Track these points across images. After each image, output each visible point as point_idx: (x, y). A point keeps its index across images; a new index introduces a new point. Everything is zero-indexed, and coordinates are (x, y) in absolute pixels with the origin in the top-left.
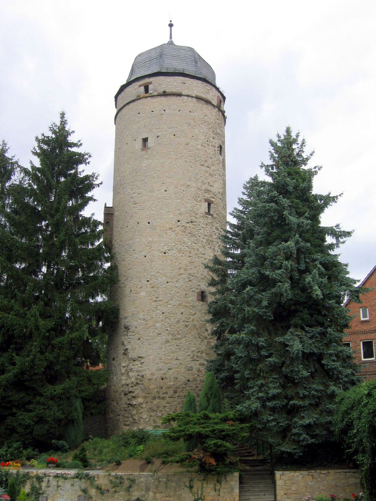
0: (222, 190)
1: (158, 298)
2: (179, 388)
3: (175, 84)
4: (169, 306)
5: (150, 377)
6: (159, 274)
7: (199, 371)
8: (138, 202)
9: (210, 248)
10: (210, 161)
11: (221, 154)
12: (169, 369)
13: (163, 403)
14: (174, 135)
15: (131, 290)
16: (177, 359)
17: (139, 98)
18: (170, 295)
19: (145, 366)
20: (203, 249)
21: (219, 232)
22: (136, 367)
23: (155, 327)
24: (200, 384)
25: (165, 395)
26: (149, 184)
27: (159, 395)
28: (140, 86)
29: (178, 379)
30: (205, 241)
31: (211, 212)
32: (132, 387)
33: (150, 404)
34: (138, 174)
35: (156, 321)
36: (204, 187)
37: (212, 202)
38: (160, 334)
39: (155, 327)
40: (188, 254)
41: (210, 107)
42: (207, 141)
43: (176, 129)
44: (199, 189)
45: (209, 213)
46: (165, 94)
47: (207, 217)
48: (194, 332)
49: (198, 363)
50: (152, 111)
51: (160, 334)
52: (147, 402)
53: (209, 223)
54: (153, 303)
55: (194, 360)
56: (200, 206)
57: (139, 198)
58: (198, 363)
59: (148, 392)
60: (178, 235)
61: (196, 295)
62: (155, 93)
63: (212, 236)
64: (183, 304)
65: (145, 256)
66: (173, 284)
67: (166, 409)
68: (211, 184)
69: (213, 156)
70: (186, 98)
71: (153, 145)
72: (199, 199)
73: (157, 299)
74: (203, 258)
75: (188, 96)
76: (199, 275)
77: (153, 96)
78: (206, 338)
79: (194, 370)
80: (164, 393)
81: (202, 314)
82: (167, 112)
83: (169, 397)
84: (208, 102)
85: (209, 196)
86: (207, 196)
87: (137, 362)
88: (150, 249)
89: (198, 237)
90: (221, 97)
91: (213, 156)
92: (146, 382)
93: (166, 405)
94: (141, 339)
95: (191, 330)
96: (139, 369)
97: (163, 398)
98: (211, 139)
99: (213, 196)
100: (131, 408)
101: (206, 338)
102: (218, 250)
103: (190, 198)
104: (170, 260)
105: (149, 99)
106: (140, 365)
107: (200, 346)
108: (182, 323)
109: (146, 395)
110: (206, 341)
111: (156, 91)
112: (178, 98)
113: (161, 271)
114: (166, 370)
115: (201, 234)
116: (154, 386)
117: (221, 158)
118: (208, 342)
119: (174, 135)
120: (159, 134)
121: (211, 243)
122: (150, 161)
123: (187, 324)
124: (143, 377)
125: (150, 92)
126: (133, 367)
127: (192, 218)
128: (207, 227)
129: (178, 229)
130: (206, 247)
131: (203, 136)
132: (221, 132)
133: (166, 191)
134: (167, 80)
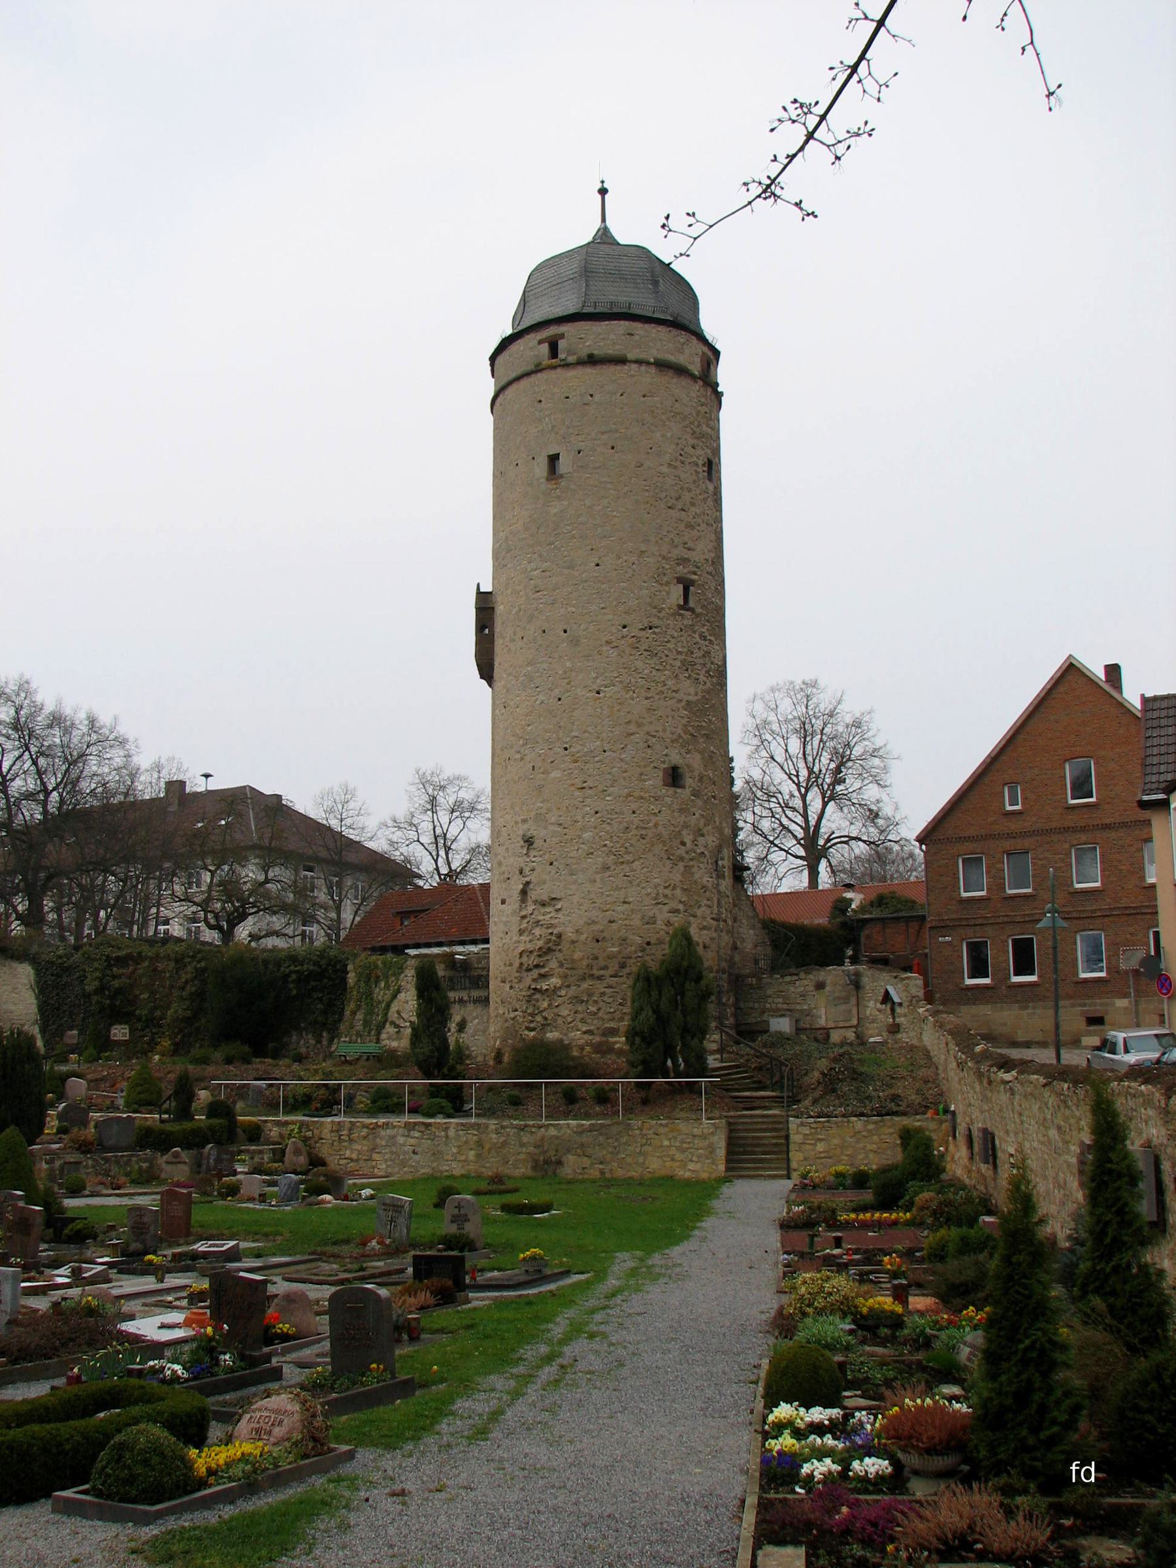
0: (713, 555)
2: (630, 958)
3: (612, 336)
4: (608, 798)
5: (573, 936)
6: (586, 735)
9: (689, 677)
10: (687, 497)
11: (710, 479)
12: (611, 922)
13: (600, 987)
14: (613, 448)
15: (533, 767)
16: (625, 902)
17: (538, 369)
18: (609, 777)
20: (674, 682)
21: (707, 643)
22: (547, 917)
23: (581, 841)
25: (602, 972)
27: (591, 972)
29: (628, 941)
30: (678, 664)
31: (691, 604)
32: (540, 956)
33: (573, 991)
34: (542, 530)
35: (583, 829)
36: (676, 553)
37: (692, 583)
38: (592, 853)
40: (644, 694)
41: (685, 381)
42: (681, 455)
43: (618, 435)
44: (664, 558)
45: (685, 606)
46: (592, 360)
47: (680, 615)
48: (659, 848)
49: (666, 908)
50: (567, 398)
51: (592, 853)
52: (568, 986)
53: (686, 626)
54: (577, 793)
55: (659, 903)
56: (668, 593)
58: (666, 908)
60: (623, 654)
61: (661, 774)
62: (571, 359)
63: (692, 653)
64: (636, 794)
65: (560, 699)
66: (615, 755)
67: (605, 998)
68: (690, 544)
69: (692, 487)
70: (634, 366)
71: (570, 470)
72: (665, 579)
75: (639, 362)
76: (668, 734)
77: (566, 365)
78: (682, 859)
79: (659, 922)
80: (602, 969)
81: (673, 811)
82: (597, 398)
83: (611, 976)
84: (680, 371)
85: (686, 571)
86: (681, 570)
87: (548, 909)
88: (568, 684)
89: (664, 658)
90: (710, 354)
91: (692, 487)
92: (565, 946)
93: (606, 990)
94: (555, 863)
95: (653, 845)
97: (600, 978)
98: (690, 450)
99: (695, 569)
100: (537, 996)
101: (682, 859)
102: (705, 679)
103: (646, 578)
104: (608, 707)
105: (559, 370)
107: (671, 876)
108: (634, 832)
110: (681, 864)
111: (574, 354)
112: (619, 368)
113: (590, 729)
114: (605, 922)
115: (670, 650)
117: (711, 487)
118: (686, 867)
119: (613, 448)
120: (581, 445)
122: (566, 503)
123: (644, 832)
125: (562, 356)
126: (541, 918)
127: (651, 620)
129: (623, 642)
131: (673, 446)
132: (709, 430)
133: (598, 565)
134: (594, 328)
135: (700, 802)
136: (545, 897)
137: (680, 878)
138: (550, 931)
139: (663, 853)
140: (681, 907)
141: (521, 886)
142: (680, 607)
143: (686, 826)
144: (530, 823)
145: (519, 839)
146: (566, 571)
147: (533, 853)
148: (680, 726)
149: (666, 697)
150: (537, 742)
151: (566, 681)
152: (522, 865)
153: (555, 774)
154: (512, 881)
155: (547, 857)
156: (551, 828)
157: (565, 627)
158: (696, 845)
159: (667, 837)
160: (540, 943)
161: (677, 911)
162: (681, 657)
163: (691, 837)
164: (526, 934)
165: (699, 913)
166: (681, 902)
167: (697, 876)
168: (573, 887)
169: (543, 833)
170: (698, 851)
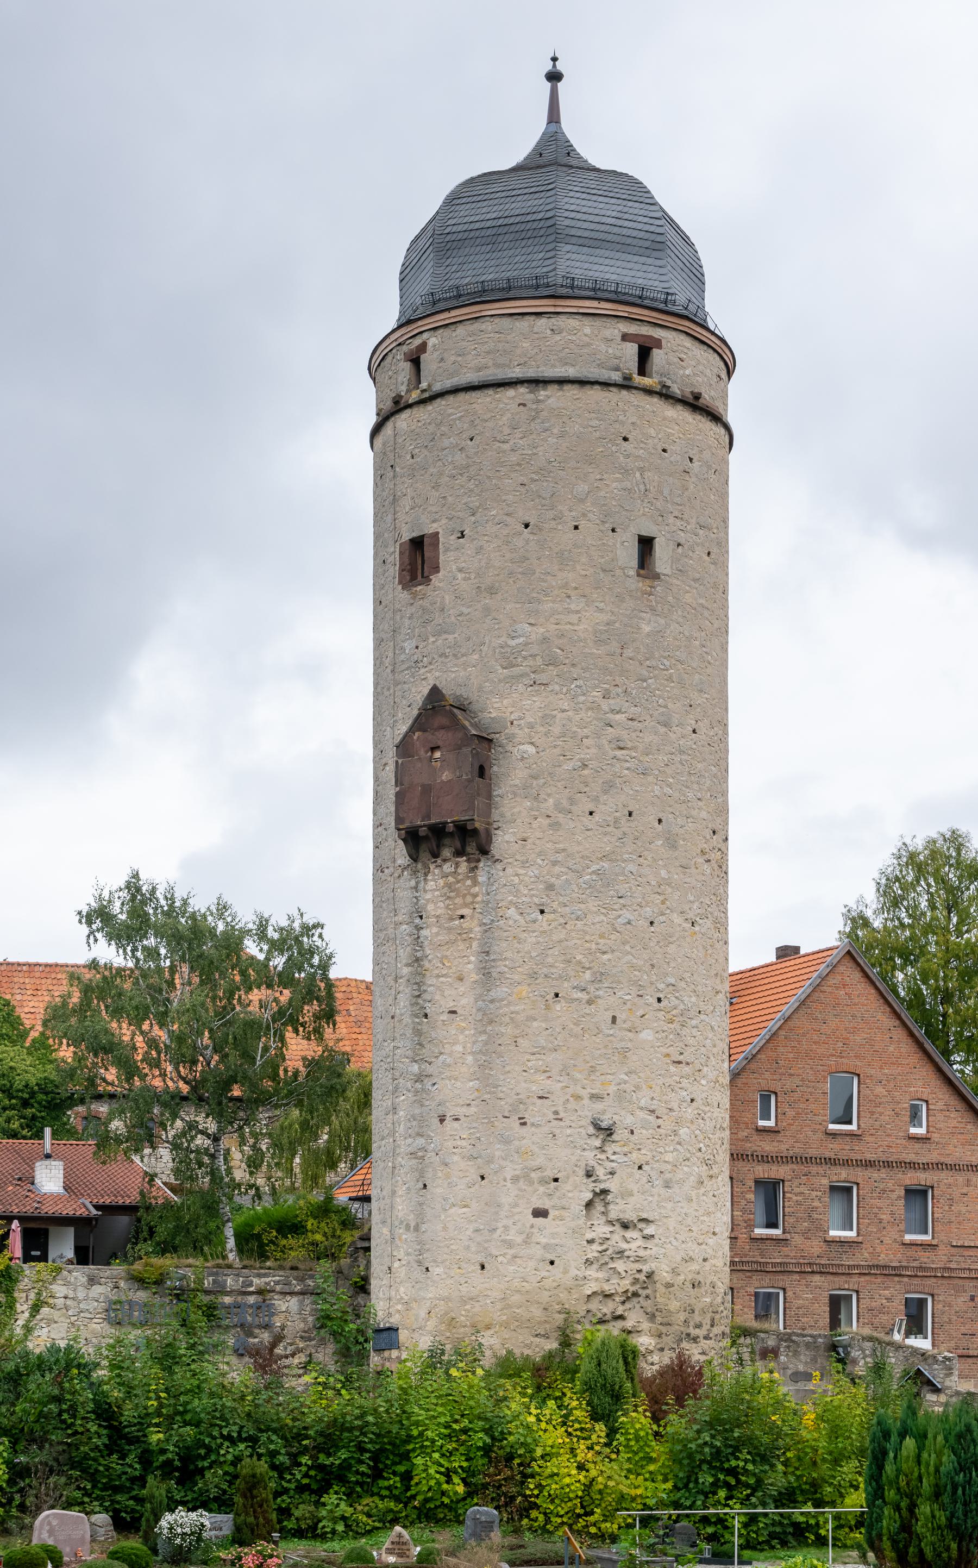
1: (681, 1054)
6: (683, 984)
8: (629, 745)
17: (626, 385)
19: (656, 1245)
22: (633, 1245)
23: (677, 1139)
26: (660, 697)
28: (625, 337)
34: (628, 652)
38: (688, 1160)
39: (677, 1139)
50: (664, 451)
52: (662, 1350)
54: (673, 1069)
57: (634, 735)
59: (665, 1320)
65: (652, 923)
73: (681, 1058)
87: (629, 1234)
88: (663, 902)
94: (645, 1167)
96: (642, 1253)
97: (695, 1340)
105: (655, 400)
106: (640, 1242)
109: (660, 1327)
116: (678, 1304)
124: (650, 1276)
126: (624, 1246)
136: (631, 1216)
138: (638, 1266)
141: (589, 1196)
144: (608, 1101)
145: (586, 1122)
146: (662, 730)
147: (610, 1148)
150: (620, 982)
151: (662, 898)
152: (592, 1163)
153: (647, 1035)
154: (565, 1187)
155: (635, 1155)
156: (642, 1115)
157: (660, 815)
160: (626, 1284)
164: (595, 1266)
168: (669, 1205)
169: (629, 1120)
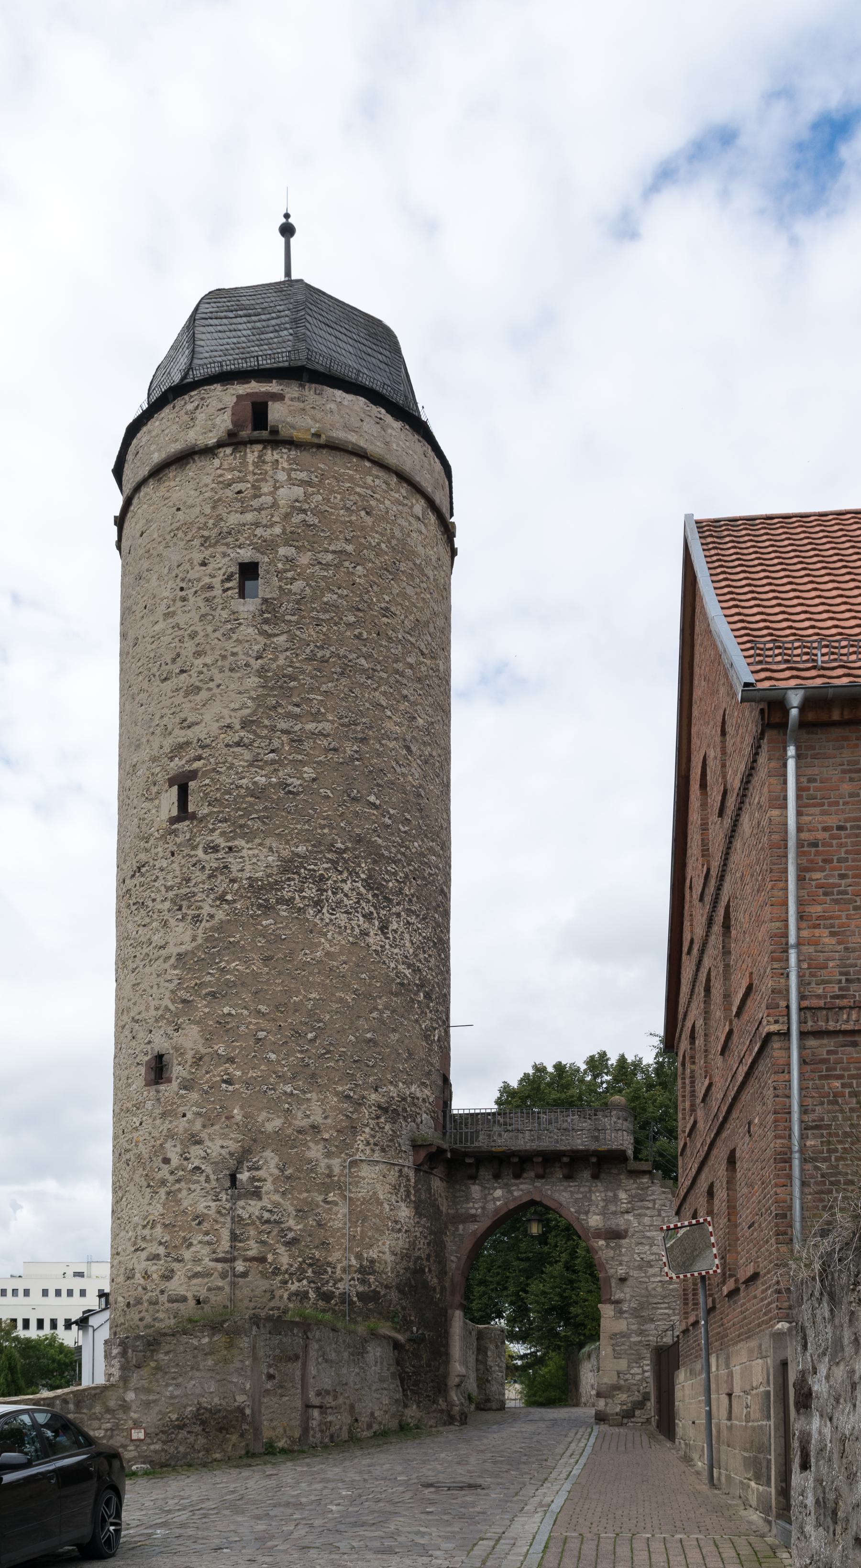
7: (147, 1276)
9: (183, 919)
24: (147, 1311)
30: (167, 905)
49: (144, 1255)
58: (144, 1255)
74: (161, 960)
85: (183, 762)
101: (163, 1182)
121: (185, 904)
128: (173, 862)
130: (172, 922)
135: (194, 1096)
137: (161, 1210)
139: (143, 1179)
140: (161, 1250)
142: (173, 821)
143: (171, 1135)
148: (168, 994)
149: (151, 960)
158: (186, 1159)
159: (147, 1156)
161: (156, 1257)
162: (171, 894)
163: (178, 1149)
165: (187, 1255)
166: (161, 1243)
167: (185, 1203)
170: (190, 1167)
